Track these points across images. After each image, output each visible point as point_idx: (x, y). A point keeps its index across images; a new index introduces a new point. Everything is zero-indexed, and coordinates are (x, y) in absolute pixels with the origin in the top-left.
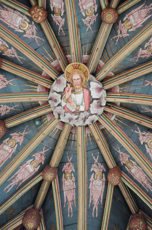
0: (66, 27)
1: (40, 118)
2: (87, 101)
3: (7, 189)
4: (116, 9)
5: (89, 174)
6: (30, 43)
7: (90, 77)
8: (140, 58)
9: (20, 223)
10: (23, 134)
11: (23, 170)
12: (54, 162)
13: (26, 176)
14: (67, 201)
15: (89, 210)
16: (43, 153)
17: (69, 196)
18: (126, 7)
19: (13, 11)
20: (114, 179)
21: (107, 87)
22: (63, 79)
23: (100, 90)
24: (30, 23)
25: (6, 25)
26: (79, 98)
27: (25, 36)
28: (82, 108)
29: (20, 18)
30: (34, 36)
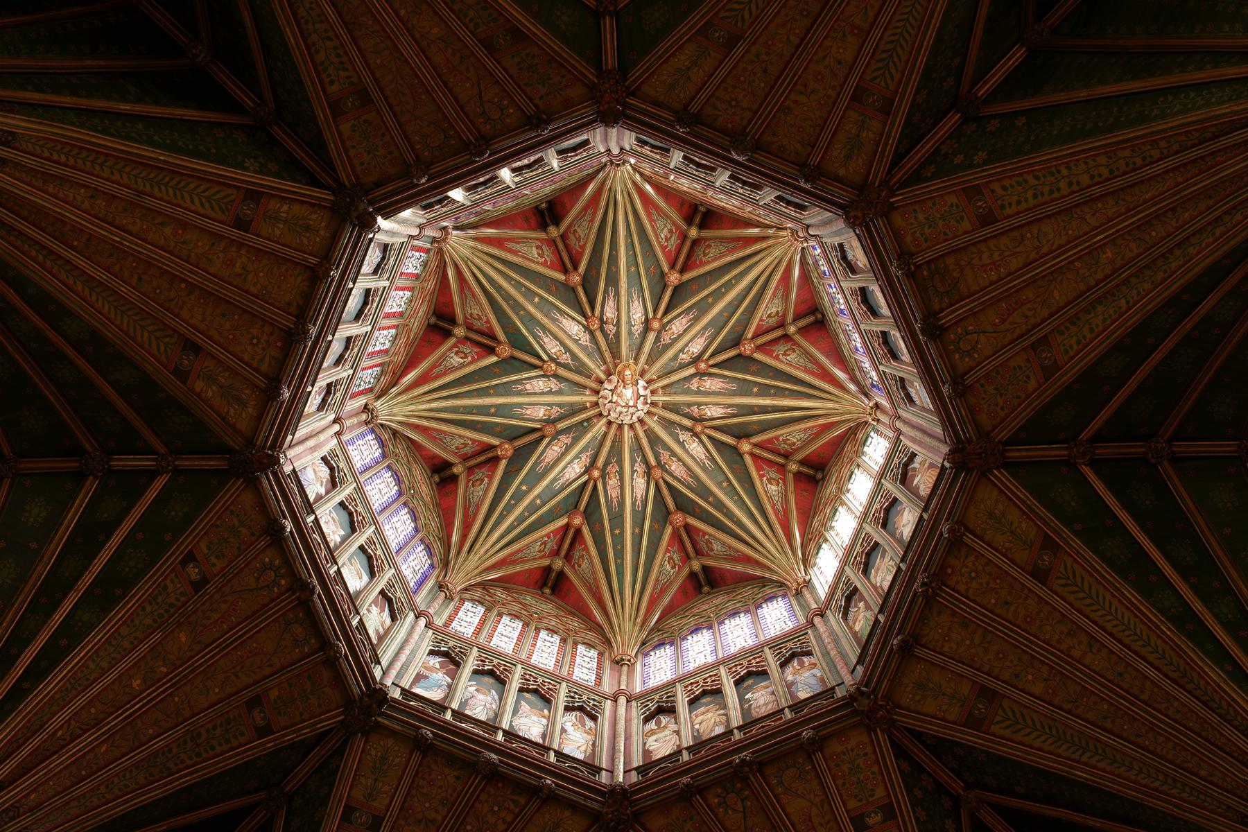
0: (617, 335)
1: (588, 420)
2: (635, 396)
4: (661, 319)
5: (633, 472)
6: (584, 348)
7: (637, 377)
9: (566, 520)
11: (570, 470)
12: (600, 463)
13: (573, 476)
14: (612, 498)
15: (634, 504)
16: (588, 454)
17: (614, 494)
18: (670, 317)
21: (652, 387)
22: (614, 378)
23: (646, 388)
24: (584, 332)
25: (565, 332)
28: (631, 403)
30: (588, 343)
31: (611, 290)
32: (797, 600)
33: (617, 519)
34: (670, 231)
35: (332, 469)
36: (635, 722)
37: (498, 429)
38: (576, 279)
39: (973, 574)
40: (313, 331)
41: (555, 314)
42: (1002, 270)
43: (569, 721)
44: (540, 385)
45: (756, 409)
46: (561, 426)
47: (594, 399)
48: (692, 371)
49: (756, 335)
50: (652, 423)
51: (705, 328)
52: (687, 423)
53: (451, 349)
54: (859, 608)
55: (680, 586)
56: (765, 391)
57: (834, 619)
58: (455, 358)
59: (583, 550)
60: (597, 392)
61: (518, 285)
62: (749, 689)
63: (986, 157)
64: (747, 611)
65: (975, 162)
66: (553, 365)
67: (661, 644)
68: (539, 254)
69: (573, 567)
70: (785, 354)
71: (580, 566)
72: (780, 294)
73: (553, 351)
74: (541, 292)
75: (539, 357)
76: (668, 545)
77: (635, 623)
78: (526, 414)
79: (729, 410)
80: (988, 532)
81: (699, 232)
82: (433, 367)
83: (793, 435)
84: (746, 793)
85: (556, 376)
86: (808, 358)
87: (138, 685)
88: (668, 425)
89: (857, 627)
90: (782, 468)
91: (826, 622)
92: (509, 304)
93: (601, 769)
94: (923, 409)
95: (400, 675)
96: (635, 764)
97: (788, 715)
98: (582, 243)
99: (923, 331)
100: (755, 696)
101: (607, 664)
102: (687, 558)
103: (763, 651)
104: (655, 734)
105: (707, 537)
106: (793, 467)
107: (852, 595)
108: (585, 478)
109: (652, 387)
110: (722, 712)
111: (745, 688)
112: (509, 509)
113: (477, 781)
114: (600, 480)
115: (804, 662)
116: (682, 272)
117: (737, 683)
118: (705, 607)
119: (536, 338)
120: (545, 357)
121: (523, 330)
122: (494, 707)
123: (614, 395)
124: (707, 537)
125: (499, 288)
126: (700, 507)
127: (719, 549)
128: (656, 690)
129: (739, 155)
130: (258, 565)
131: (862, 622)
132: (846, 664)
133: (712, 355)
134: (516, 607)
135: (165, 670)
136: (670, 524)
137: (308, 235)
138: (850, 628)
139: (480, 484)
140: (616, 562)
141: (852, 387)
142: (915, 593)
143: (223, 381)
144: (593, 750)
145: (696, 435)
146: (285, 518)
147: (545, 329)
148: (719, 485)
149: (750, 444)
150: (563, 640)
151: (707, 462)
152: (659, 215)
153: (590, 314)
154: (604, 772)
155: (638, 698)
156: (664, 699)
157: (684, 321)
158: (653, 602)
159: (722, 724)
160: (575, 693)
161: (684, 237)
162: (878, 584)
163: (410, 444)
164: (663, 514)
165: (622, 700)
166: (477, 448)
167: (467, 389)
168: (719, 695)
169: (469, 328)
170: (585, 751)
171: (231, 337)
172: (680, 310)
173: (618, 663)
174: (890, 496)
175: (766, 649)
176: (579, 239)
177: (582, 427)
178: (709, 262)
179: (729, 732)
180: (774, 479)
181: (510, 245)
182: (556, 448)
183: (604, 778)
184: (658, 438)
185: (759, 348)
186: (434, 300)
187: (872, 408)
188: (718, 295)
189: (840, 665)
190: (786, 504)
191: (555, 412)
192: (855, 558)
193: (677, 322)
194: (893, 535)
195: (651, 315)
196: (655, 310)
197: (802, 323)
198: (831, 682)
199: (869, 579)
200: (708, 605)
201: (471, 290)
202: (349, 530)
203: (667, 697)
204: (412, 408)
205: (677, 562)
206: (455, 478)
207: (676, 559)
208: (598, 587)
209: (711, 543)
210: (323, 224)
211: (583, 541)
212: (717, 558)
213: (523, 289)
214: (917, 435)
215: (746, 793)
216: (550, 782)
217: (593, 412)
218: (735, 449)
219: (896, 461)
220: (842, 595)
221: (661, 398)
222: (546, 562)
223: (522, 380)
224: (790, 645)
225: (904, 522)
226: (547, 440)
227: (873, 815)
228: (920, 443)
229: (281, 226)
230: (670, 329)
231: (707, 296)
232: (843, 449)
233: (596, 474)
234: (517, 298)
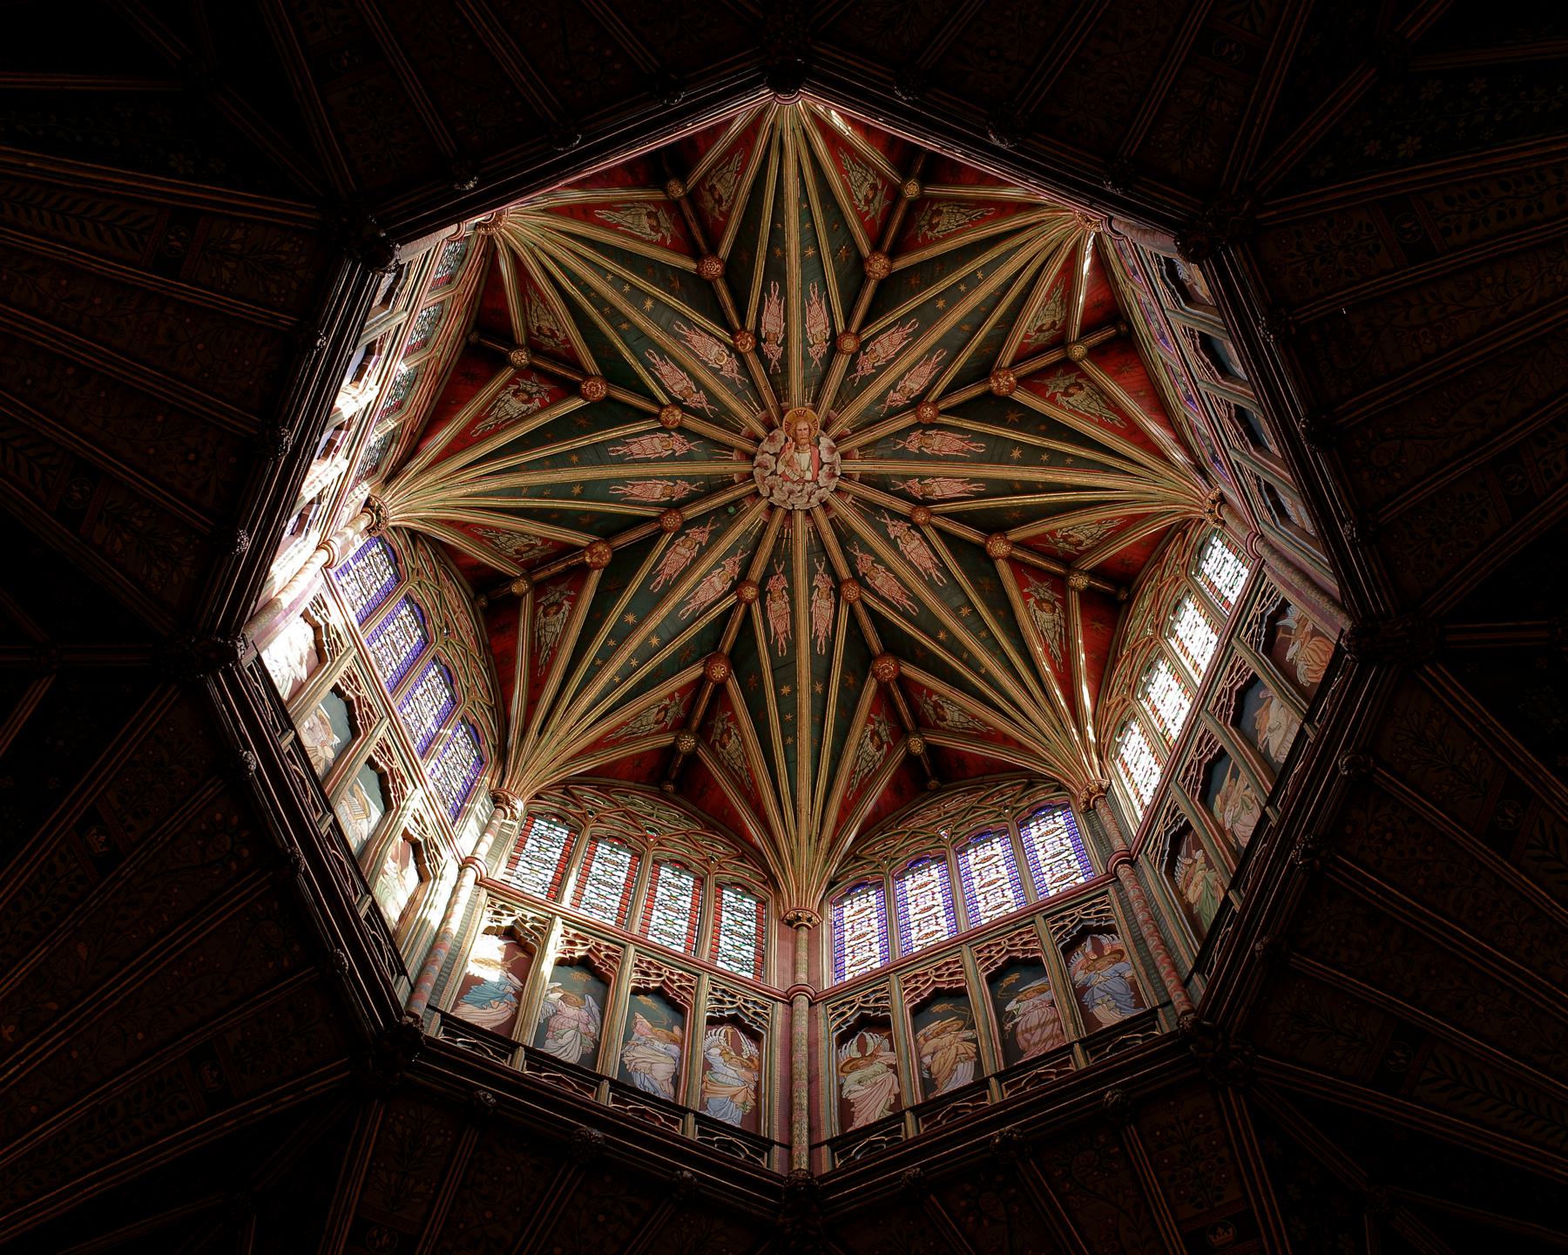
0: (784, 361)
1: (736, 503)
2: (815, 464)
3: (683, 615)
4: (858, 334)
5: (811, 589)
6: (729, 384)
8: (890, 407)
9: (701, 671)
10: (708, 529)
12: (756, 573)
13: (712, 596)
14: (776, 633)
15: (813, 643)
16: (737, 559)
17: (780, 626)
18: (872, 331)
19: (707, 336)
20: (852, 592)
21: (844, 448)
22: (780, 434)
23: (832, 451)
24: (729, 356)
25: (697, 357)
26: (804, 458)
27: (722, 373)
28: (809, 476)
29: (717, 348)
31: (775, 287)
32: (1088, 821)
33: (785, 669)
34: (874, 187)
35: (316, 629)
36: (823, 1045)
37: (585, 520)
38: (714, 268)
39: (1388, 836)
40: (289, 439)
41: (679, 327)
42: (1443, 336)
43: (714, 1044)
44: (654, 445)
45: (1017, 486)
46: (691, 513)
47: (745, 467)
48: (908, 420)
49: (1017, 361)
50: (844, 509)
51: (931, 351)
52: (902, 507)
53: (505, 386)
54: (1195, 861)
55: (892, 778)
56: (1032, 456)
57: (1151, 874)
58: (514, 401)
59: (729, 719)
60: (750, 457)
61: (618, 282)
62: (1012, 992)
63: (1419, 147)
64: (1002, 833)
65: (1401, 154)
66: (677, 412)
67: (861, 884)
68: (652, 227)
69: (712, 747)
70: (1066, 394)
71: (723, 746)
72: (1058, 294)
73: (677, 388)
74: (656, 291)
75: (653, 399)
76: (871, 711)
77: (817, 850)
78: (632, 495)
79: (972, 487)
80: (1413, 767)
81: (922, 189)
82: (477, 420)
83: (1080, 528)
84: (1013, 1191)
85: (681, 430)
86: (1104, 402)
87: (10, 1034)
88: (870, 510)
89: (1192, 895)
90: (1060, 584)
91: (1138, 879)
92: (602, 313)
93: (773, 1143)
94: (1303, 533)
95: (438, 989)
96: (825, 1136)
97: (1080, 1061)
98: (724, 208)
99: (1311, 437)
100: (1023, 1005)
101: (775, 925)
102: (900, 733)
103: (1033, 922)
104: (858, 1068)
105: (935, 698)
106: (1080, 582)
107: (1180, 836)
108: (731, 600)
109: (844, 448)
110: (968, 1034)
111: (1006, 990)
112: (606, 655)
113: (570, 1175)
114: (757, 603)
115: (1102, 947)
116: (893, 255)
117: (993, 980)
118: (932, 814)
119: (648, 366)
120: (664, 399)
121: (627, 354)
122: (592, 1029)
123: (780, 463)
124: (935, 698)
125: (586, 288)
126: (924, 648)
127: (956, 718)
128: (857, 984)
129: (1002, 142)
130: (203, 827)
131: (1200, 887)
132: (1175, 967)
133: (947, 393)
134: (615, 824)
135: (55, 1007)
136: (875, 675)
137: (278, 278)
138: (1180, 894)
139: (557, 613)
140: (784, 742)
141: (1179, 456)
142: (1292, 866)
143: (140, 524)
144: (757, 1100)
145: (916, 527)
146: (248, 748)
147: (662, 352)
148: (955, 612)
149: (1007, 542)
150: (700, 881)
151: (935, 574)
152: (854, 161)
153: (738, 326)
154: (776, 1148)
155: (828, 997)
156: (871, 1004)
157: (897, 337)
158: (847, 810)
159: (970, 1058)
160: (724, 991)
161: (895, 194)
162: (1228, 826)
163: (440, 549)
164: (860, 660)
165: (802, 1003)
166: (551, 551)
167: (536, 456)
168: (961, 1001)
169: (534, 348)
170: (744, 1103)
171: (151, 451)
172: (891, 319)
173: (792, 923)
174: (1247, 671)
175: (1039, 918)
176: (719, 201)
177: (725, 517)
178: (938, 241)
179: (980, 1084)
180: (1047, 601)
181: (603, 214)
182: (682, 551)
183: (775, 1161)
184: (852, 532)
185: (1025, 382)
186: (477, 306)
187: (1214, 502)
188: (953, 296)
189: (1164, 969)
190: (1068, 645)
191: (681, 490)
192: (1188, 769)
193: (883, 338)
194: (1251, 742)
195: (840, 327)
196: (848, 317)
197: (1095, 339)
198: (1151, 1000)
199: (1210, 812)
200: (939, 816)
201: (537, 290)
202: (347, 733)
203: (877, 1000)
204: (444, 495)
205: (885, 738)
206: (516, 600)
207: (883, 734)
208: (754, 783)
209: (942, 708)
210: (303, 259)
211: (728, 705)
212: (952, 732)
213: (627, 288)
214: (1295, 580)
215: (1013, 1191)
216: (689, 1175)
217: (744, 490)
218: (981, 551)
219: (1256, 610)
220: (1166, 833)
221: (858, 467)
222: (667, 740)
223: (625, 437)
224: (1078, 912)
225: (1272, 723)
226: (668, 537)
227: (1220, 1230)
228: (1299, 594)
229: (232, 265)
230: (873, 351)
231: (937, 297)
232: (1163, 553)
233: (750, 592)
234: (617, 305)
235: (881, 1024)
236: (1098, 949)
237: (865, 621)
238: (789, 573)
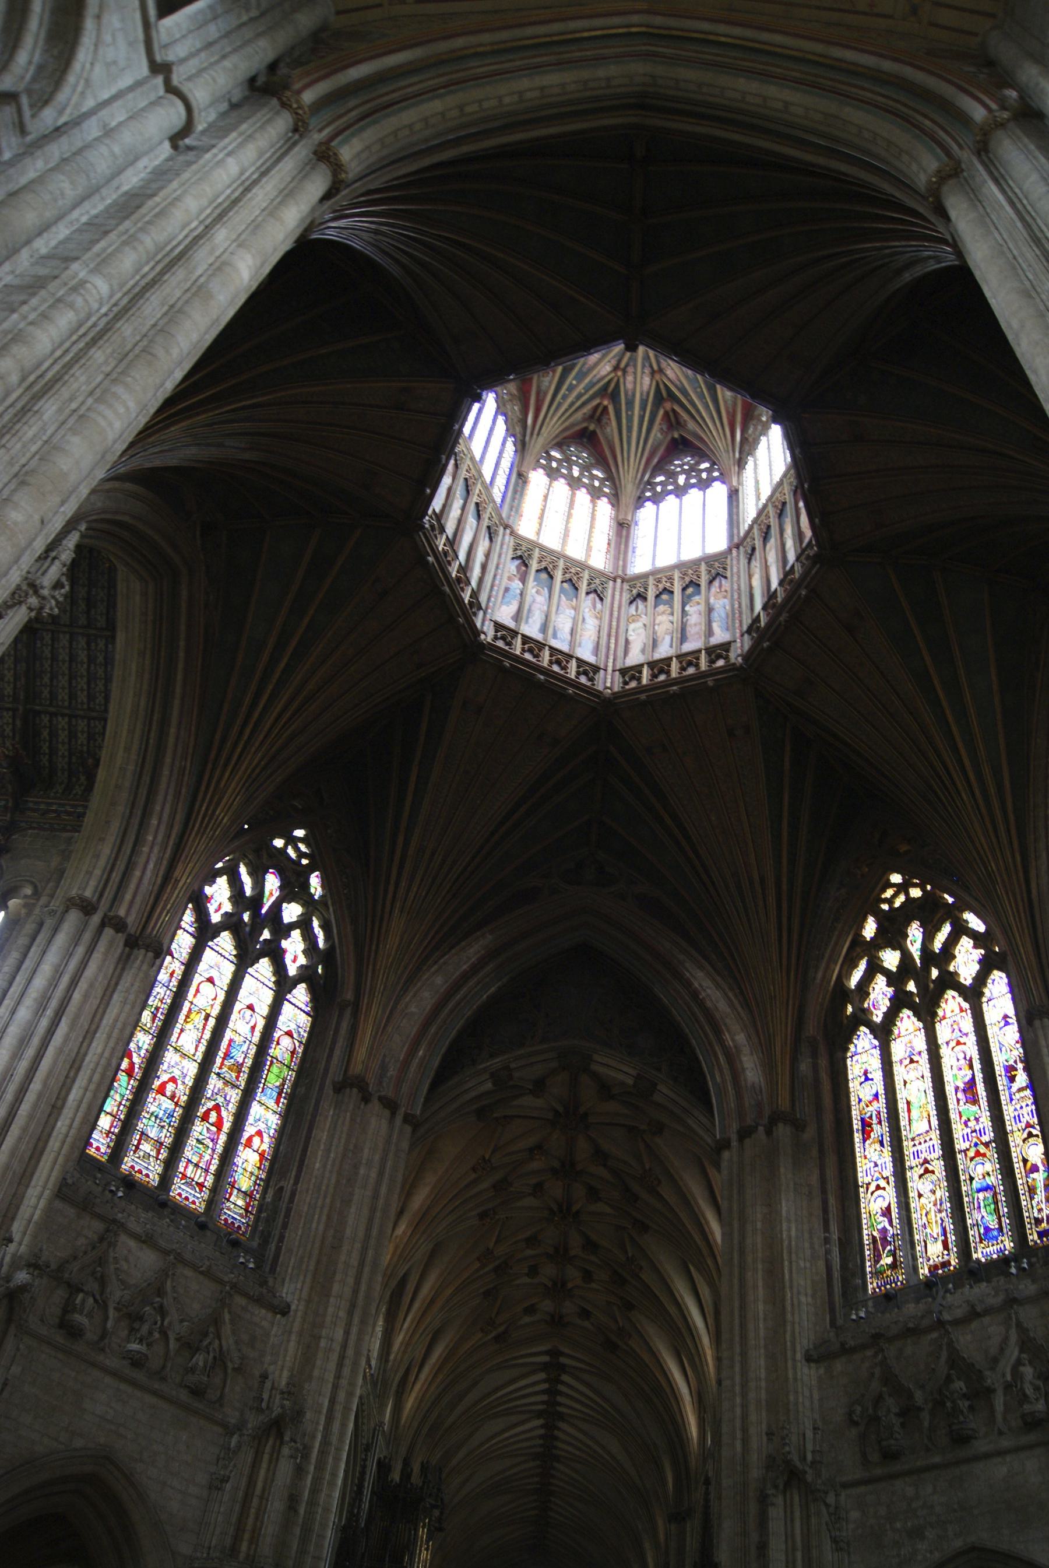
5: (643, 373)
12: (622, 365)
15: (642, 394)
17: (630, 386)
33: (630, 404)
96: (618, 668)
102: (671, 427)
108: (613, 375)
112: (565, 397)
142: (780, 624)
155: (628, 581)
164: (659, 399)
211: (608, 413)
222: (585, 425)
235: (645, 599)
236: (720, 586)
237: (662, 386)
238: (635, 366)
